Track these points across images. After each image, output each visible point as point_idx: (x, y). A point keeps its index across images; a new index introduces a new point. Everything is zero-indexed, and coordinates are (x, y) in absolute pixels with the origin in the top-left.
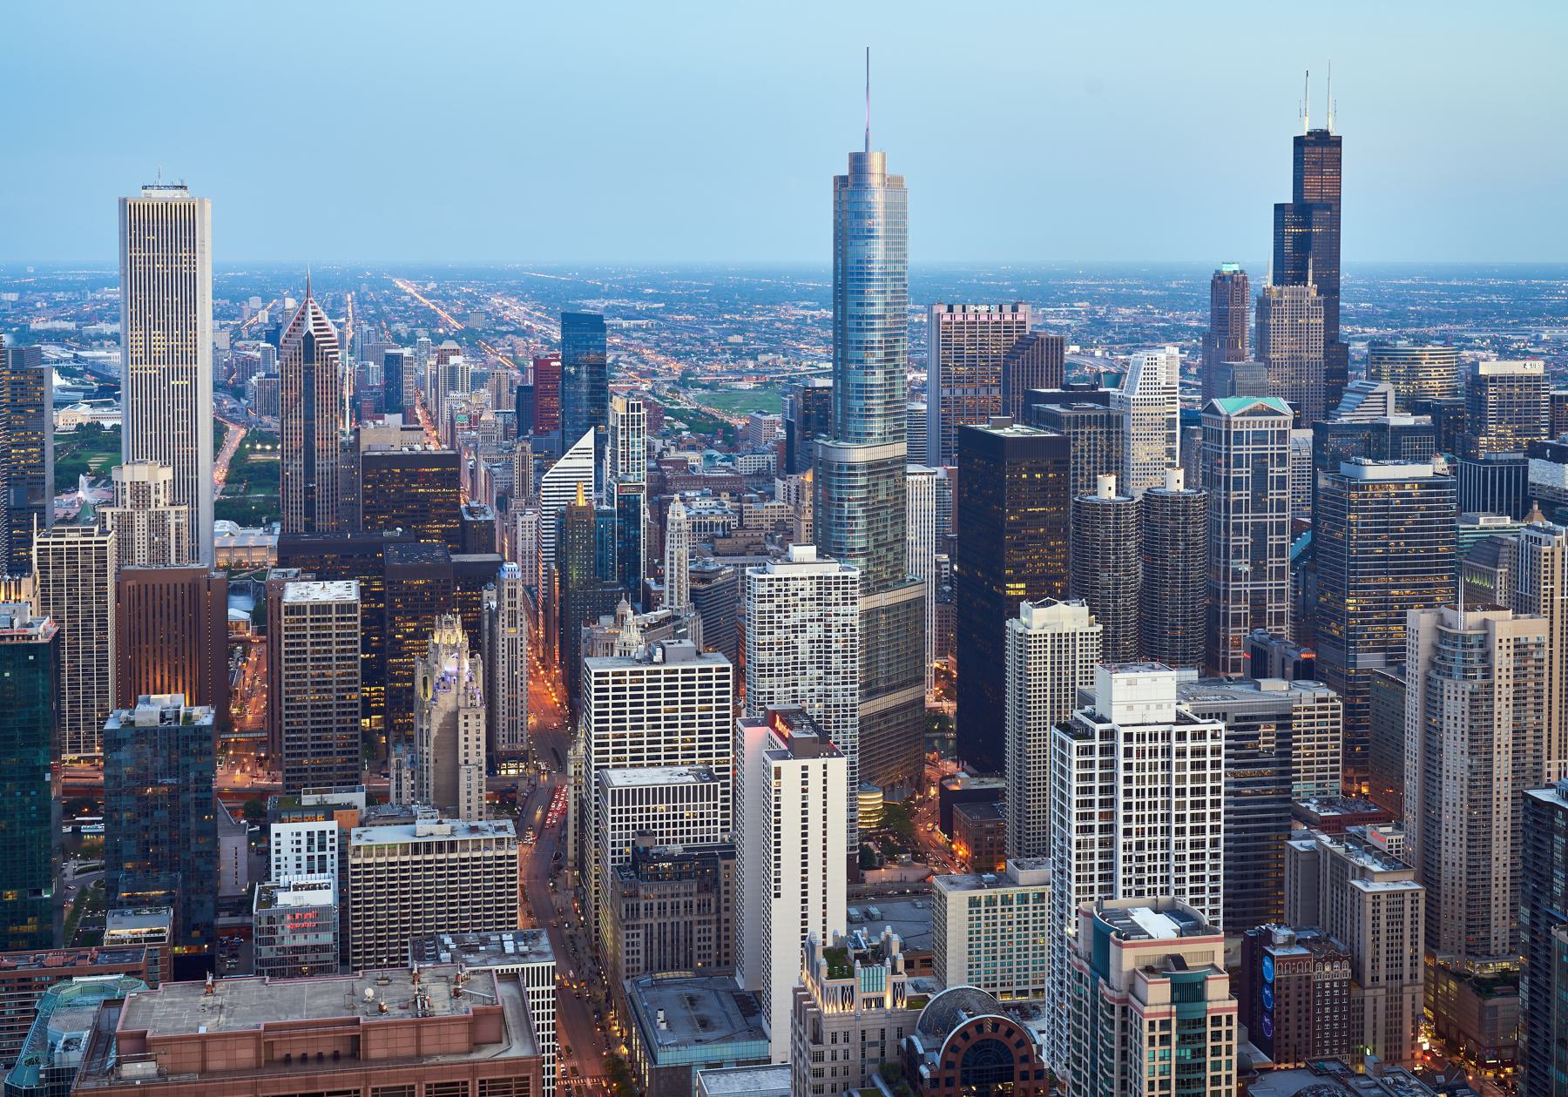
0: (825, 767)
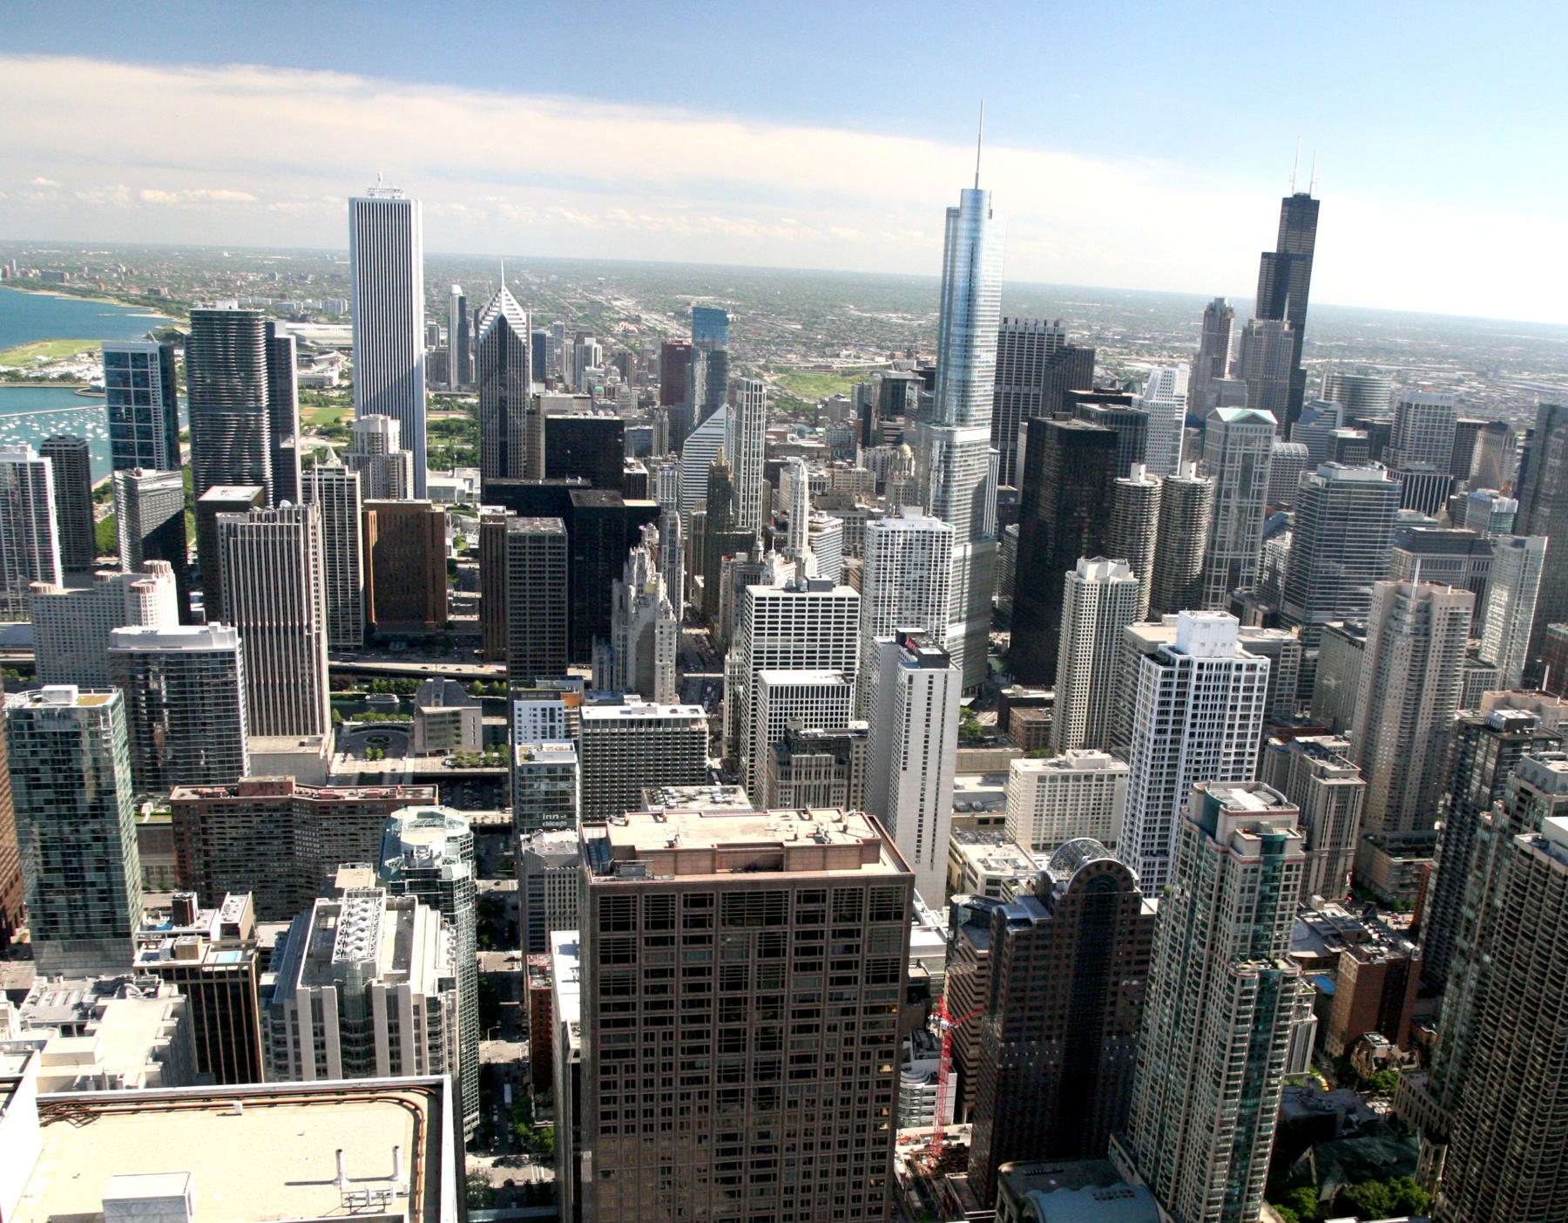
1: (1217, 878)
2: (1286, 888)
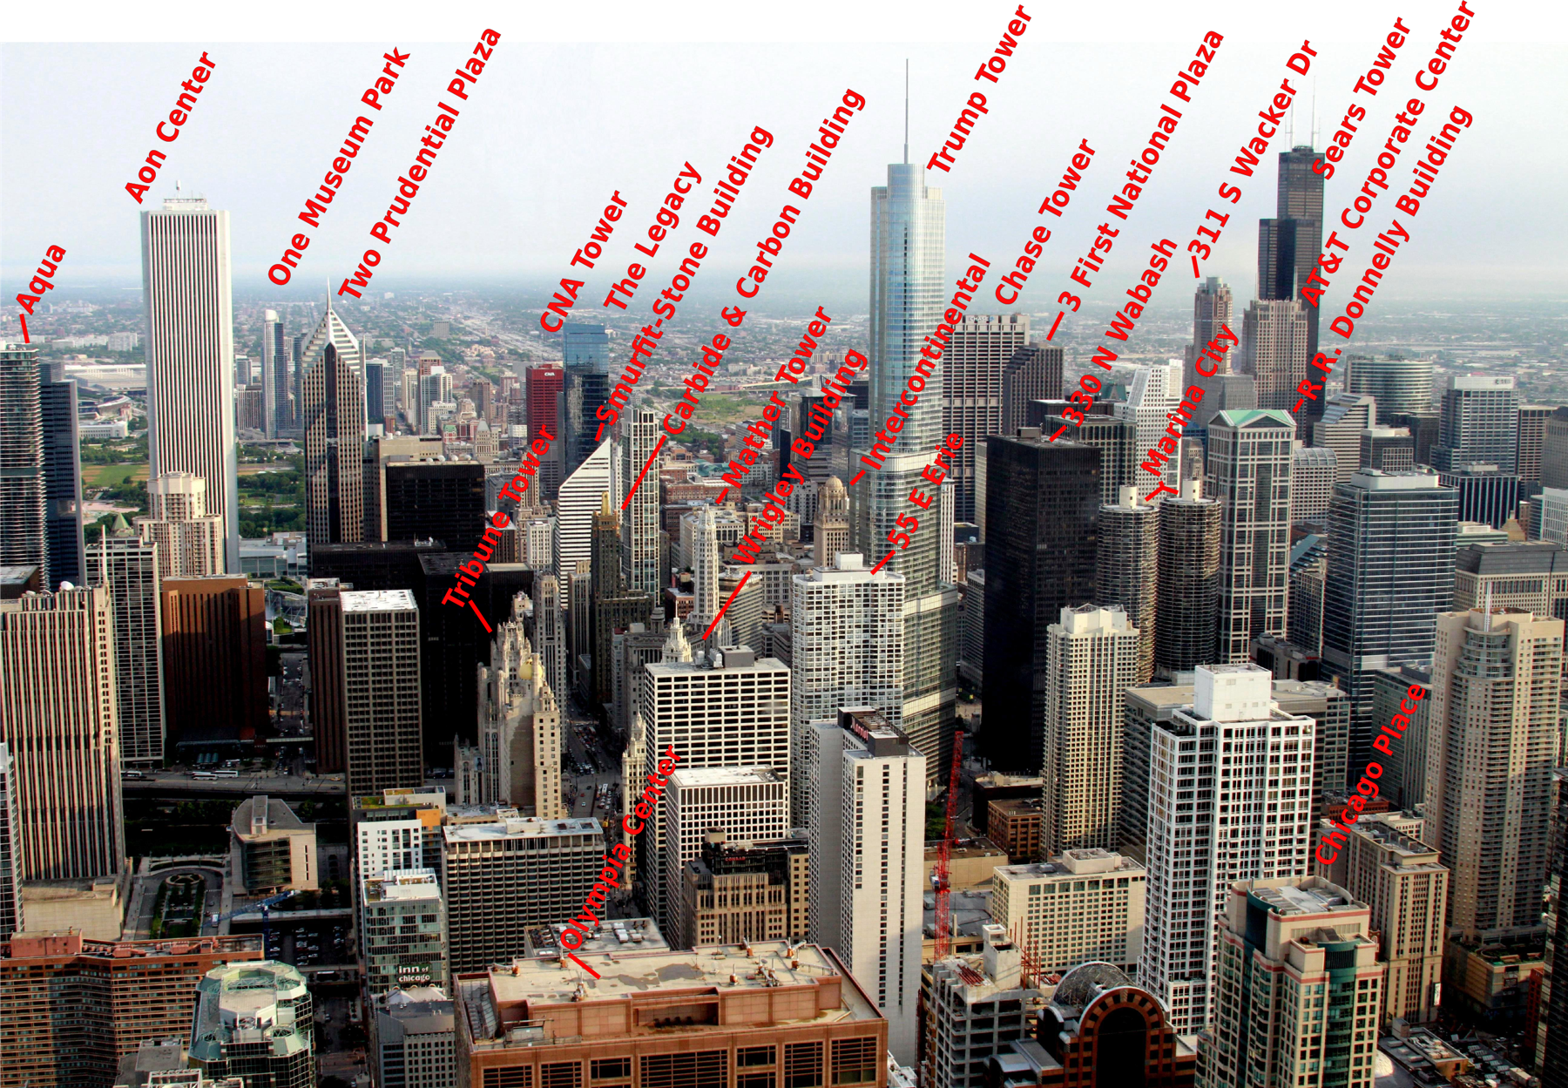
0: (886, 767)
1: (1271, 1003)
2: (1362, 1010)
